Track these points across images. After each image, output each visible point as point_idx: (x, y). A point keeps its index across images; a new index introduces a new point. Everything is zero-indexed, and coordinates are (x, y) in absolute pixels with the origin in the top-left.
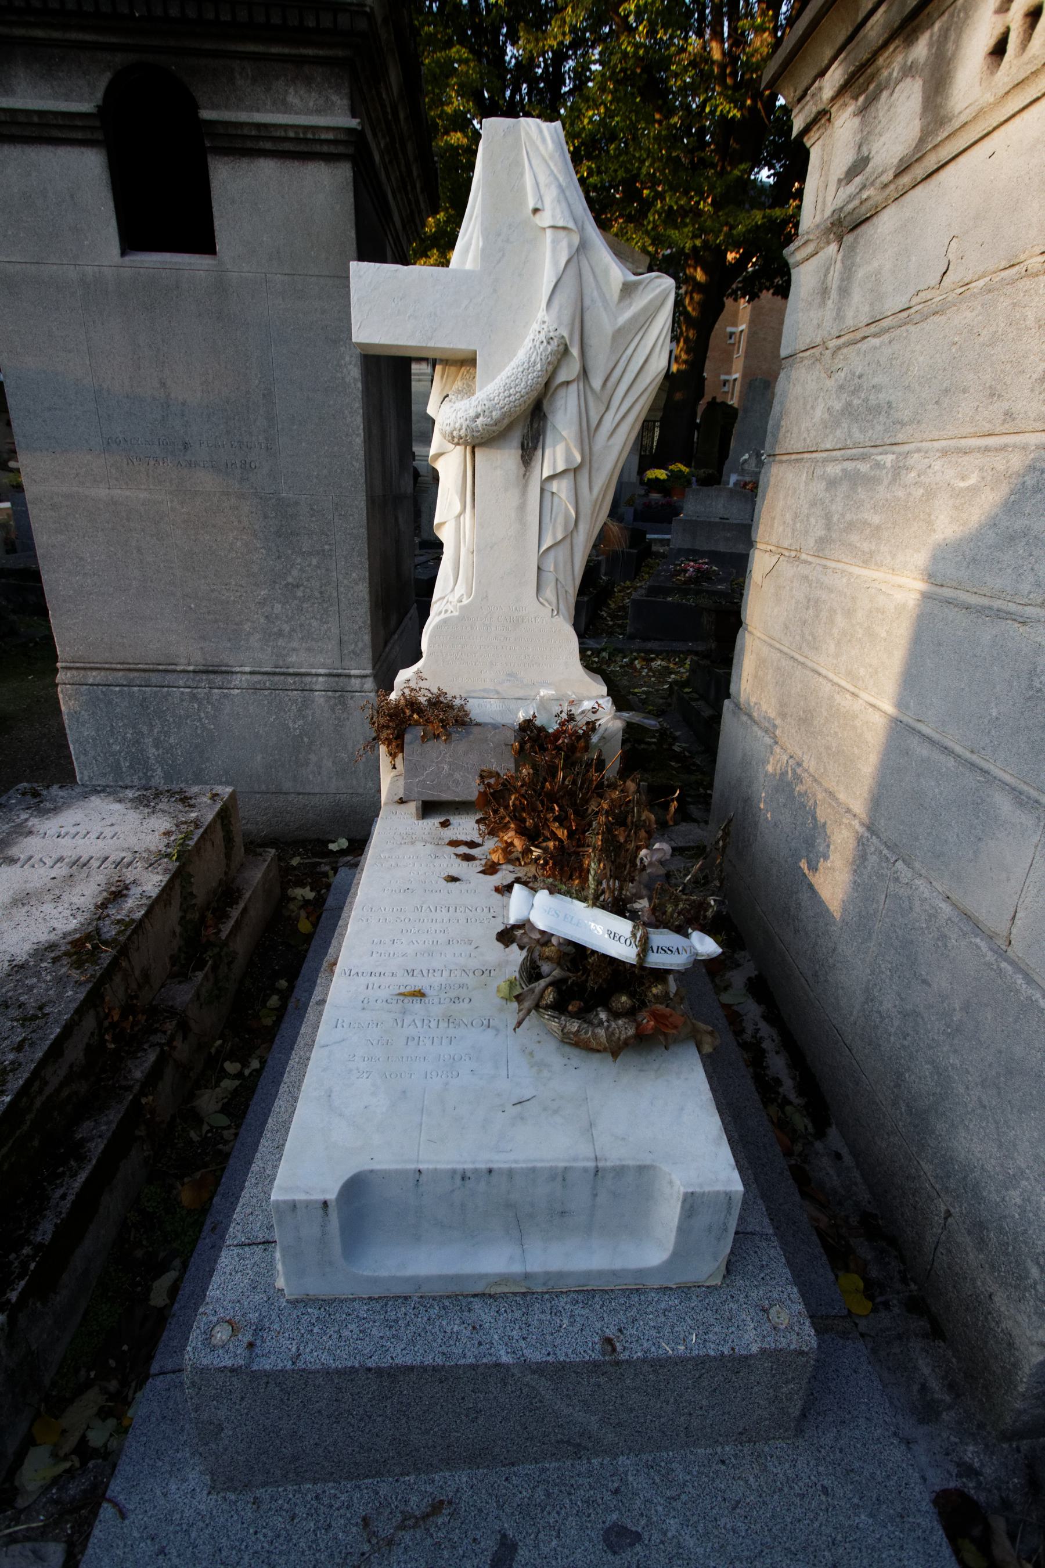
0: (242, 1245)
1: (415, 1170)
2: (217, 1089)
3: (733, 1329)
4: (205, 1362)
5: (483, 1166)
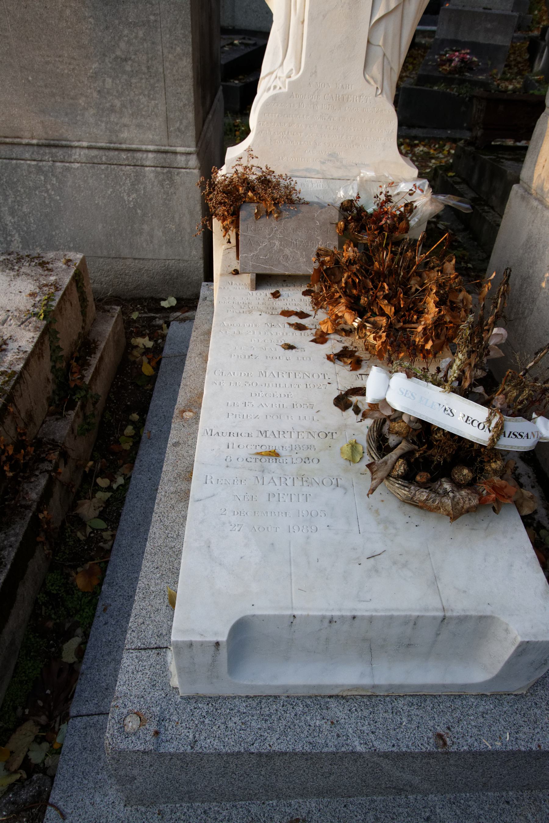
0: (140, 649)
1: (290, 616)
2: (94, 500)
3: (539, 730)
4: (122, 746)
5: (349, 614)
